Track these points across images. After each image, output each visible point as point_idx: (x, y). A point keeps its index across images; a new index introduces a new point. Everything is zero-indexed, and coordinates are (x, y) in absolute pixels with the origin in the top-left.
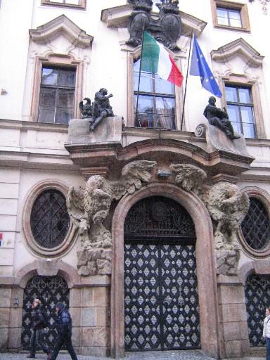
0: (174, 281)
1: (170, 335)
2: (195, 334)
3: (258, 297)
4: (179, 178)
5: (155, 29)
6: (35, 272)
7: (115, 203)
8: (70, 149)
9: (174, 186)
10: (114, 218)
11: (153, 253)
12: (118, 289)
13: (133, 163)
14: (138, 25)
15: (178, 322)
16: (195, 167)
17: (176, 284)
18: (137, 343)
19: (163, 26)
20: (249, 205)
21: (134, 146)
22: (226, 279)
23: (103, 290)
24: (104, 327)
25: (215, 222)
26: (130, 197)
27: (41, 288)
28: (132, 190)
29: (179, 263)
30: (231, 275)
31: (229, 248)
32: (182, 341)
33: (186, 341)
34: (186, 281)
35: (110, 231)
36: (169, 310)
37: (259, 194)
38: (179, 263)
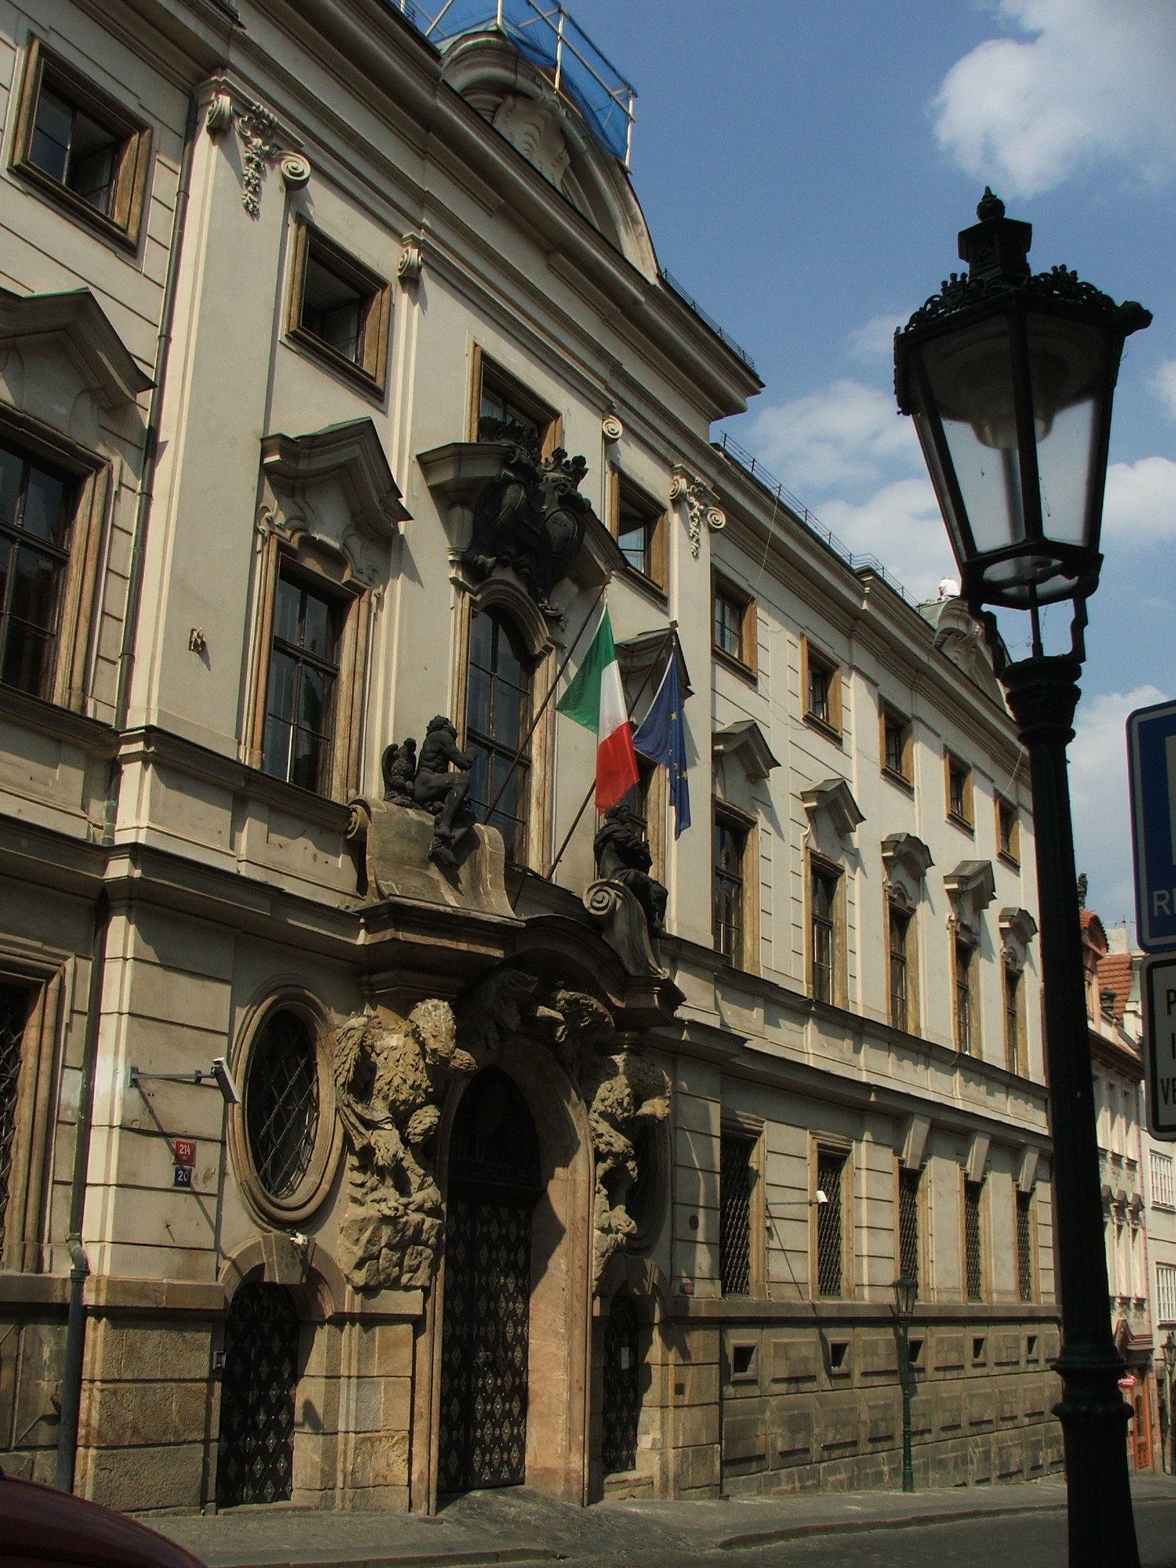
33: (502, 1463)
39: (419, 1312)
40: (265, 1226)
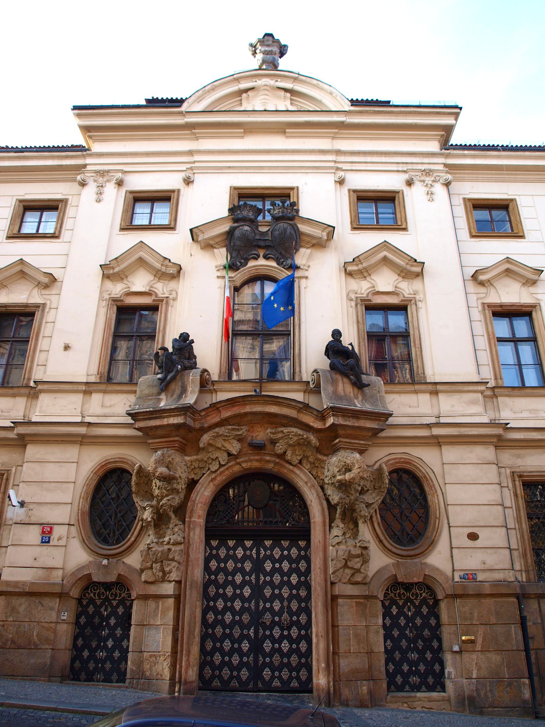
0: (277, 591)
1: (267, 669)
2: (303, 670)
3: (406, 617)
4: (280, 448)
5: (262, 244)
6: (89, 576)
7: (192, 484)
8: (133, 415)
9: (273, 459)
10: (189, 504)
11: (248, 553)
12: (193, 606)
13: (217, 430)
14: (238, 243)
15: (280, 650)
16: (300, 432)
17: (280, 597)
18: (220, 677)
19: (273, 239)
20: (387, 481)
21: (215, 407)
22: (350, 590)
23: (171, 601)
24: (169, 653)
25: (332, 508)
26: (213, 476)
27: (100, 598)
28: (214, 467)
29: (286, 566)
30: (357, 583)
31: (350, 546)
32: (285, 677)
33: (291, 678)
34: (294, 592)
35: (184, 522)
36: (268, 633)
37: (409, 463)
38: (286, 566)
39: (177, 593)
40: (95, 557)
